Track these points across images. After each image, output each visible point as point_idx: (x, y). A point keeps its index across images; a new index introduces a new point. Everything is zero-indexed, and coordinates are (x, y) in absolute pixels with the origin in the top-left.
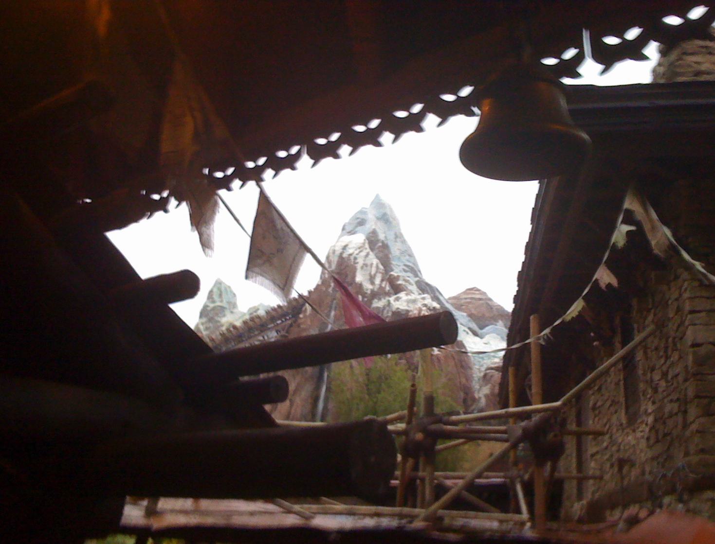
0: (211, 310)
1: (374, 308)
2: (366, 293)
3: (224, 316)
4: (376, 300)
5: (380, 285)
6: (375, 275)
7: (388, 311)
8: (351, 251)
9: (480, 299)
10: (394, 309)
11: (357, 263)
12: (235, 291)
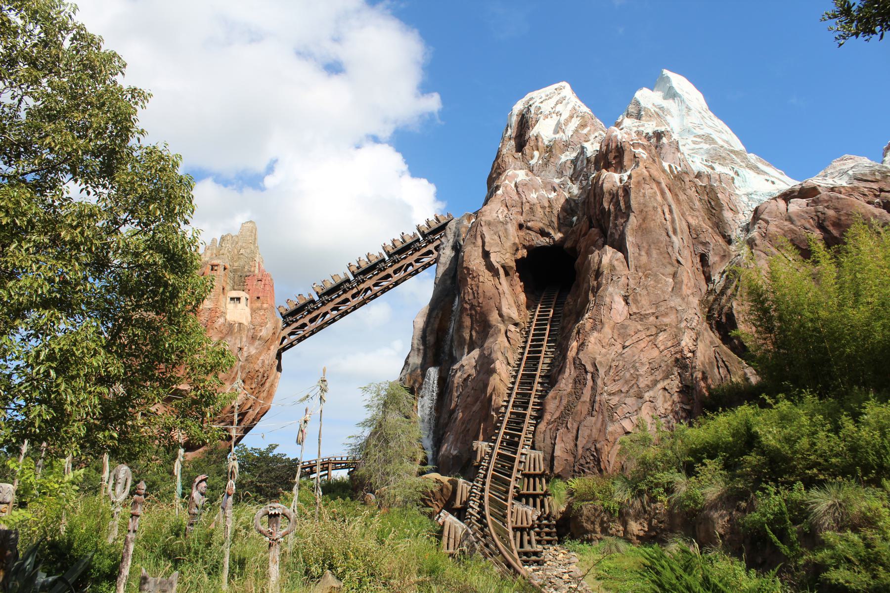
4: (568, 153)
5: (576, 131)
6: (567, 122)
7: (582, 161)
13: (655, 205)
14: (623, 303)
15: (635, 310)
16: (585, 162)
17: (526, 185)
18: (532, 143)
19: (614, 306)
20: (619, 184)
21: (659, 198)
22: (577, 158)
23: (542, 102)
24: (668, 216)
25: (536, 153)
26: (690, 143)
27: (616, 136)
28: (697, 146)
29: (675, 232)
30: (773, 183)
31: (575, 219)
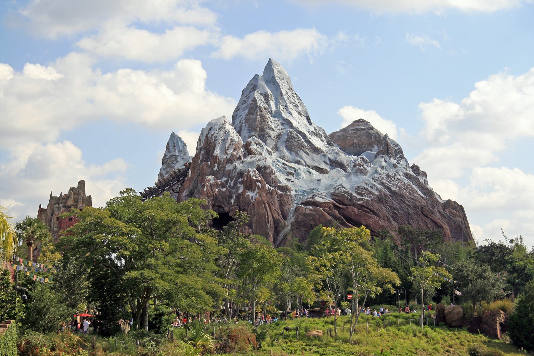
0: (168, 158)
1: (226, 171)
2: (221, 162)
3: (177, 162)
7: (235, 172)
8: (212, 133)
9: (363, 129)
10: (238, 171)
11: (217, 140)
12: (185, 142)
13: (263, 213)
16: (236, 173)
21: (264, 210)
22: (233, 170)
23: (217, 134)
24: (267, 217)
25: (216, 165)
27: (251, 175)
29: (268, 223)
31: (232, 201)
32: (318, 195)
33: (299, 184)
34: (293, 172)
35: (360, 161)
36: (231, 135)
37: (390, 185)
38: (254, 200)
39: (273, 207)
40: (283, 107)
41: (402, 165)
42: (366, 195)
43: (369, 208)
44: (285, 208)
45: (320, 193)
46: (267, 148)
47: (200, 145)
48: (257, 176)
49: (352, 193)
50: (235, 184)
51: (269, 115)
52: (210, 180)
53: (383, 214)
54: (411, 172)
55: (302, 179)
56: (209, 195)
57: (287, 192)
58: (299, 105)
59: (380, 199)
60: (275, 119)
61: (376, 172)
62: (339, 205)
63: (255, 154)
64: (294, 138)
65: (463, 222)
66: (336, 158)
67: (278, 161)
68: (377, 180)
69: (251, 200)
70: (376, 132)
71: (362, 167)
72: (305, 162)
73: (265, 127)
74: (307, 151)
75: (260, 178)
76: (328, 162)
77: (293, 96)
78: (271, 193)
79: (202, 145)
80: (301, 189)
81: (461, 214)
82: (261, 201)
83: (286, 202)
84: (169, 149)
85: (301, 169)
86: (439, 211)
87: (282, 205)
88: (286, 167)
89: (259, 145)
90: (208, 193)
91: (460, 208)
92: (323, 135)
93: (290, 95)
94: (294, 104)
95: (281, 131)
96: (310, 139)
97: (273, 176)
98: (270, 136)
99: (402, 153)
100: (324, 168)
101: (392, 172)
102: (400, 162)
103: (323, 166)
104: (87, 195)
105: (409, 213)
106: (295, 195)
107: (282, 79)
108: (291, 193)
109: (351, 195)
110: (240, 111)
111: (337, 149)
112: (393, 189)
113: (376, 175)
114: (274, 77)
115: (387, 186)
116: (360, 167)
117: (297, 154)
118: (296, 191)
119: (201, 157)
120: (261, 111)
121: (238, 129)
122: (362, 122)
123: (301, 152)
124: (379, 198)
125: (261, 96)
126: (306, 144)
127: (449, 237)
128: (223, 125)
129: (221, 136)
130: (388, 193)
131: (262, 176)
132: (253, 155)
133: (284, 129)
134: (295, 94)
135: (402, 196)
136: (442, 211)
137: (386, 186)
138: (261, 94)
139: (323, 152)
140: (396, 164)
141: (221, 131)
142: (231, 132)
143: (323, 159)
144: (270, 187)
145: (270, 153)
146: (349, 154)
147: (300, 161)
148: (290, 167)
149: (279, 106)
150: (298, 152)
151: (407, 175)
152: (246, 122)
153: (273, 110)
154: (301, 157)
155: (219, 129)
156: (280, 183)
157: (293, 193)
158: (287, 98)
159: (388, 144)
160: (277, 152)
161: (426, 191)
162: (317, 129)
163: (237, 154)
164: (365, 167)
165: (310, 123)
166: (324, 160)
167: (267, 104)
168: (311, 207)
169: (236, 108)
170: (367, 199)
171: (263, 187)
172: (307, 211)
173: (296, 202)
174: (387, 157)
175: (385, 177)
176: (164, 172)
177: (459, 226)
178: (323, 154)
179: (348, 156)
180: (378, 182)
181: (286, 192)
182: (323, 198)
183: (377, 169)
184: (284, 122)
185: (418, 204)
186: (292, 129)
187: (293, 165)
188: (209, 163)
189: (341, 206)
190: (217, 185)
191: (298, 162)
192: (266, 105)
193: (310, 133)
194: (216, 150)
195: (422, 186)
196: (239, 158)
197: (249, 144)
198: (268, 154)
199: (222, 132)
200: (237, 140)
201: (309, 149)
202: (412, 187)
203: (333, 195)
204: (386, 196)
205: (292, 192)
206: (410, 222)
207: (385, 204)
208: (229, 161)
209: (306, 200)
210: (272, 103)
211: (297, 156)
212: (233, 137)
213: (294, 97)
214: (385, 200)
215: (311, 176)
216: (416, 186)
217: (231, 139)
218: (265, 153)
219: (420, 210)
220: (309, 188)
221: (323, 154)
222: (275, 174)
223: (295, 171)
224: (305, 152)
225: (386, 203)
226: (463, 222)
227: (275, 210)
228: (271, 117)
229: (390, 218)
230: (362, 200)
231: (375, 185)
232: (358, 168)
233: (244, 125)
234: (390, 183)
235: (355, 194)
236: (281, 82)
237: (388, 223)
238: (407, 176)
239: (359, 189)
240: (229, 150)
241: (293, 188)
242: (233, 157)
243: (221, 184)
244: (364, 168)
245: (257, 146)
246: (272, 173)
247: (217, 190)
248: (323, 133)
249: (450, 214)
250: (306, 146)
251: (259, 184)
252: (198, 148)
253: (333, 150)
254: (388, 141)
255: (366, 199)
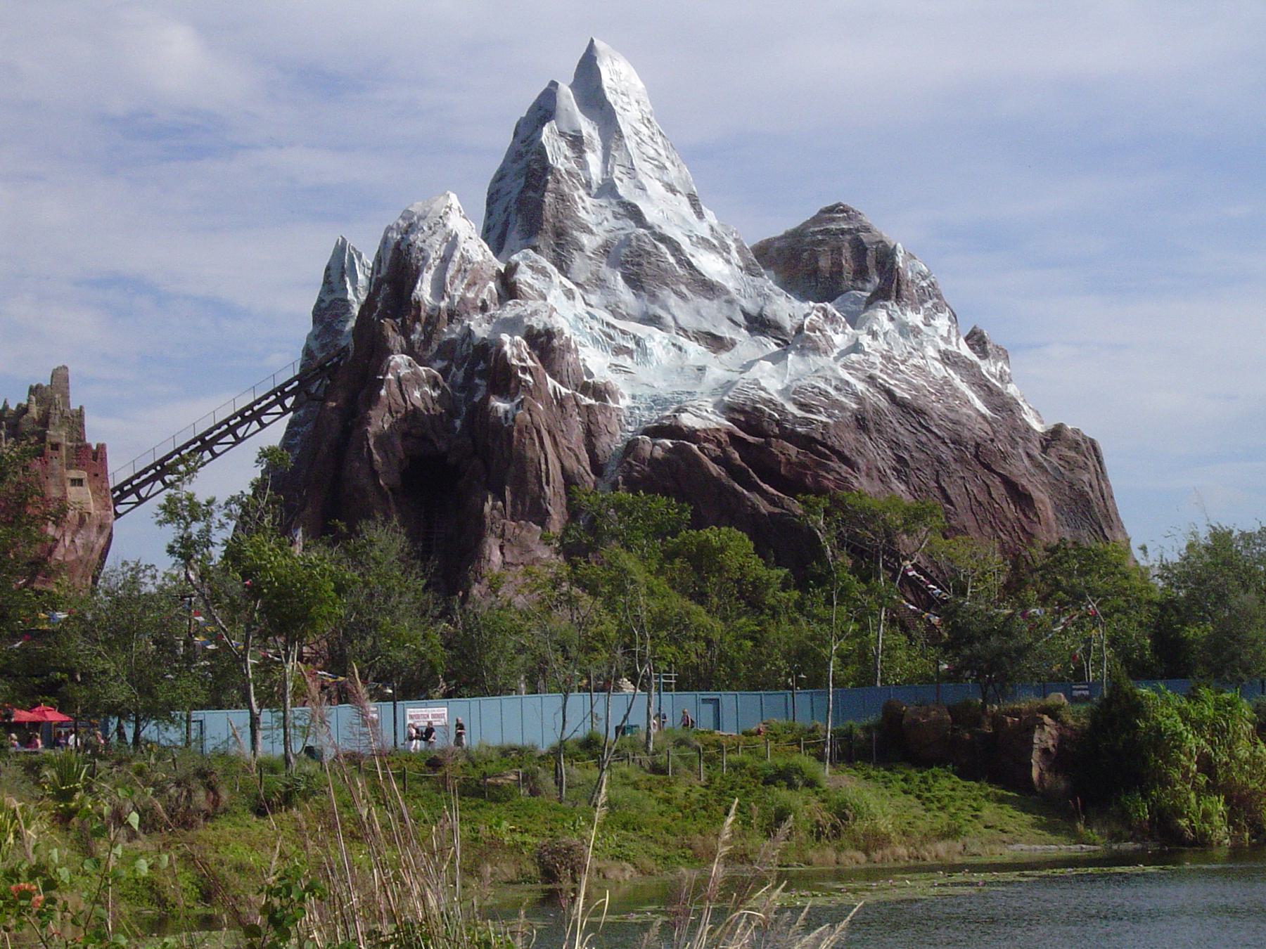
7: (468, 346)
14: (499, 553)
15: (508, 559)
17: (408, 381)
18: (413, 312)
19: (493, 558)
20: (503, 421)
22: (463, 340)
24: (543, 467)
25: (419, 327)
26: (610, 217)
28: (620, 224)
29: (548, 484)
30: (680, 349)
31: (458, 423)
32: (690, 409)
33: (645, 380)
34: (632, 345)
35: (814, 318)
36: (461, 245)
37: (892, 382)
38: (510, 423)
39: (564, 441)
40: (621, 168)
41: (936, 329)
42: (822, 410)
43: (829, 443)
44: (598, 444)
45: (696, 403)
46: (561, 282)
47: (378, 272)
48: (525, 355)
49: (782, 405)
50: (469, 377)
51: (582, 192)
52: (398, 366)
53: (868, 461)
54: (965, 350)
55: (655, 364)
56: (394, 407)
57: (606, 401)
58: (668, 164)
59: (861, 422)
60: (596, 201)
61: (856, 347)
62: (746, 436)
63: (526, 297)
64: (649, 253)
65: (1095, 483)
66: (762, 309)
67: (593, 317)
68: (857, 369)
69: (503, 421)
70: (878, 239)
71: (818, 333)
72: (674, 318)
73: (568, 223)
74: (683, 289)
75: (530, 363)
76: (740, 318)
77: (652, 139)
78: (561, 402)
79: (384, 272)
80: (648, 392)
81: (1090, 464)
82: (530, 425)
83: (602, 427)
84: (330, 283)
85: (656, 340)
86: (1028, 455)
87: (590, 436)
88: (612, 332)
89: (543, 272)
90: (392, 401)
91: (1089, 444)
92: (733, 246)
93: (645, 138)
94: (656, 163)
95: (612, 235)
96: (693, 256)
97: (570, 358)
98: (581, 249)
99: (939, 296)
100: (728, 336)
101: (900, 347)
102: (932, 321)
103: (725, 331)
104: (74, 406)
105: (939, 460)
106: (628, 407)
107: (623, 94)
108: (618, 403)
109: (782, 411)
110: (508, 180)
111: (768, 283)
112: (898, 393)
113: (854, 357)
114: (599, 89)
115: (884, 386)
116: (812, 334)
117: (653, 297)
118: (634, 397)
119: (379, 305)
120: (558, 182)
121: (497, 231)
122: (842, 211)
123: (665, 292)
124: (857, 419)
125: (559, 139)
126: (681, 271)
127: (1047, 524)
128: (441, 217)
129: (435, 251)
130: (884, 403)
131: (541, 359)
132: (521, 298)
133: (623, 229)
134: (660, 133)
135: (920, 412)
136: (1036, 452)
137: (881, 384)
138: (562, 134)
139: (728, 292)
140: (918, 327)
141: (434, 233)
142: (461, 238)
143: (726, 310)
144: (558, 385)
145: (569, 295)
146: (804, 297)
147: (660, 317)
148: (623, 332)
149: (612, 167)
150: (658, 292)
151: (948, 358)
152: (519, 210)
153: (594, 178)
154: (665, 308)
155: (430, 228)
156: (590, 375)
157: (624, 403)
158: (634, 145)
159: (898, 273)
160: (599, 292)
161: (997, 401)
162: (719, 229)
163: (477, 296)
164: (830, 333)
165: (700, 215)
166: (729, 314)
167: (577, 163)
168: (668, 442)
169: (498, 172)
170: (824, 419)
171: (540, 385)
172: (658, 453)
173: (631, 428)
174: (896, 308)
175: (878, 360)
176: (315, 345)
177: (1082, 494)
178: (726, 297)
179: (797, 303)
180: (859, 374)
181: (605, 400)
182: (703, 418)
183: (857, 339)
184: (621, 211)
185: (966, 434)
186: (641, 231)
187: (632, 327)
188: (399, 320)
189: (750, 439)
190: (417, 380)
191: (652, 320)
192: (572, 165)
193: (694, 239)
194: (418, 286)
195: (988, 387)
196: (484, 308)
197: (512, 269)
198: (564, 298)
199: (438, 239)
200: (480, 258)
201: (687, 285)
202: (957, 389)
203: (730, 410)
204: (877, 411)
205: (621, 401)
206: (943, 484)
207: (874, 435)
208: (452, 315)
209: (656, 422)
210: (594, 160)
211: (653, 303)
212: (468, 251)
213: (656, 143)
214: (876, 423)
215: (680, 358)
216: (972, 384)
217: (462, 255)
218: (555, 297)
219: (972, 450)
220: (670, 390)
221: (726, 297)
222: (577, 350)
223: (638, 344)
224: (676, 293)
225: (879, 431)
226: (1095, 483)
227: (569, 449)
228: (586, 198)
229: (888, 471)
230: (809, 422)
231: (847, 383)
232: (808, 337)
233: (512, 217)
234: (892, 378)
235: (791, 408)
236: (620, 103)
237: (881, 485)
238: (948, 359)
239: (803, 393)
240: (455, 286)
241: (626, 391)
242: (465, 305)
243: (428, 377)
244: (824, 335)
245: (535, 276)
246: (567, 347)
247: (417, 394)
248: (736, 240)
249: (1061, 462)
250: (679, 276)
251: (528, 378)
252: (373, 280)
253: (754, 287)
254: (901, 265)
255: (822, 422)
